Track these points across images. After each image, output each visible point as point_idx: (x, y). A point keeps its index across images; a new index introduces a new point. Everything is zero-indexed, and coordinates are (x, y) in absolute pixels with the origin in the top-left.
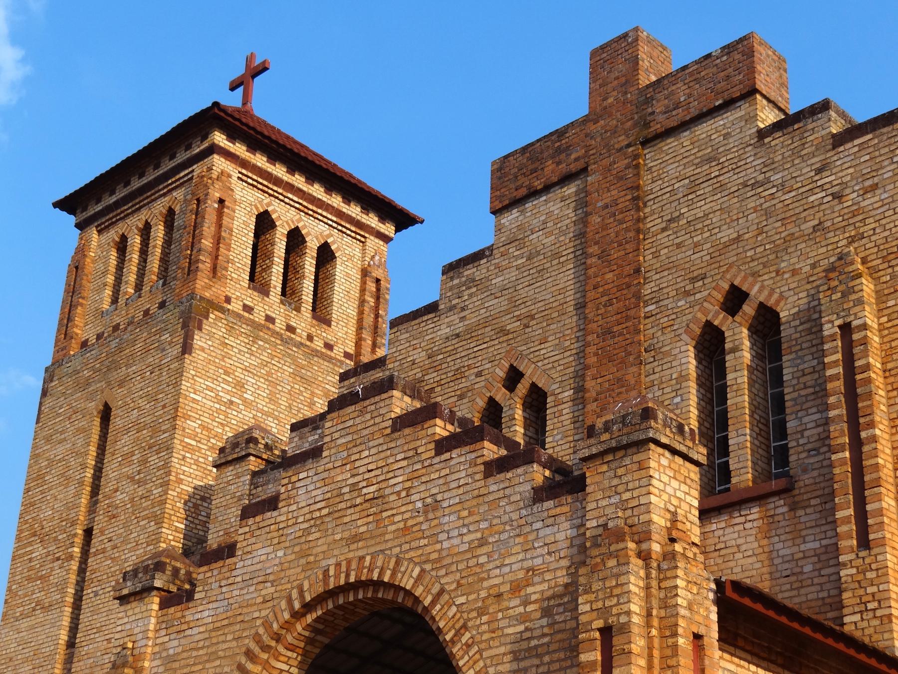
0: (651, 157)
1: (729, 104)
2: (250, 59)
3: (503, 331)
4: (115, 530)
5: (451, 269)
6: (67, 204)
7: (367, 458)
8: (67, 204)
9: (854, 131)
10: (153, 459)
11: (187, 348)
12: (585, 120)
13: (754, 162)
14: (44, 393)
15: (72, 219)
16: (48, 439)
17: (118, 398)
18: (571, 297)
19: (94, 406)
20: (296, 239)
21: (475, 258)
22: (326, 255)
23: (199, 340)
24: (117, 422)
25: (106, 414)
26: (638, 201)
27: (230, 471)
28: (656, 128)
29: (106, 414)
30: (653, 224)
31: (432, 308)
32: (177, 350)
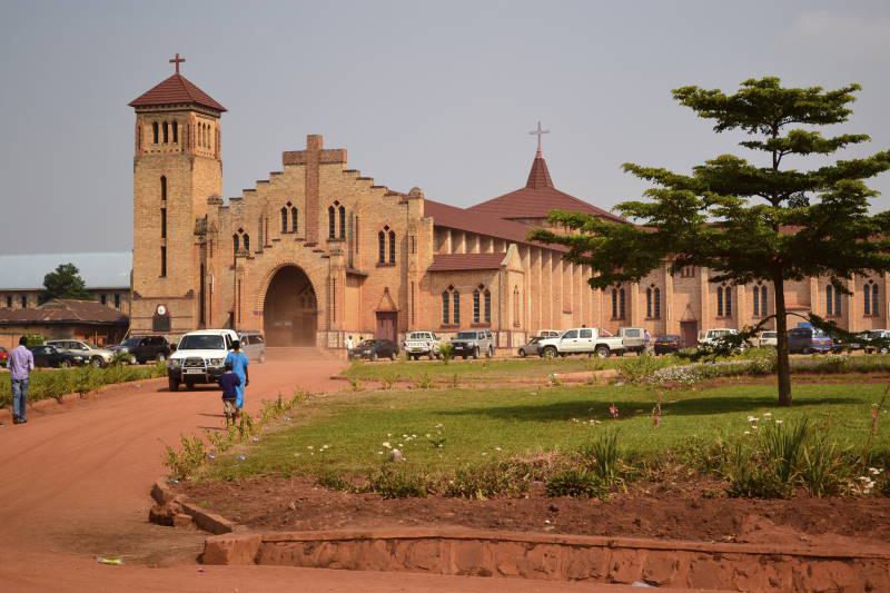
0: (320, 167)
1: (337, 162)
3: (286, 193)
5: (273, 174)
6: (132, 105)
8: (132, 105)
9: (360, 179)
10: (186, 197)
11: (192, 169)
12: (305, 151)
13: (341, 177)
14: (135, 165)
15: (133, 109)
16: (141, 179)
17: (167, 176)
18: (303, 191)
19: (159, 175)
20: (204, 126)
21: (279, 173)
22: (209, 127)
23: (194, 166)
24: (169, 183)
25: (164, 179)
26: (318, 176)
27: (212, 206)
28: (323, 160)
29: (164, 179)
30: (321, 182)
31: (268, 182)
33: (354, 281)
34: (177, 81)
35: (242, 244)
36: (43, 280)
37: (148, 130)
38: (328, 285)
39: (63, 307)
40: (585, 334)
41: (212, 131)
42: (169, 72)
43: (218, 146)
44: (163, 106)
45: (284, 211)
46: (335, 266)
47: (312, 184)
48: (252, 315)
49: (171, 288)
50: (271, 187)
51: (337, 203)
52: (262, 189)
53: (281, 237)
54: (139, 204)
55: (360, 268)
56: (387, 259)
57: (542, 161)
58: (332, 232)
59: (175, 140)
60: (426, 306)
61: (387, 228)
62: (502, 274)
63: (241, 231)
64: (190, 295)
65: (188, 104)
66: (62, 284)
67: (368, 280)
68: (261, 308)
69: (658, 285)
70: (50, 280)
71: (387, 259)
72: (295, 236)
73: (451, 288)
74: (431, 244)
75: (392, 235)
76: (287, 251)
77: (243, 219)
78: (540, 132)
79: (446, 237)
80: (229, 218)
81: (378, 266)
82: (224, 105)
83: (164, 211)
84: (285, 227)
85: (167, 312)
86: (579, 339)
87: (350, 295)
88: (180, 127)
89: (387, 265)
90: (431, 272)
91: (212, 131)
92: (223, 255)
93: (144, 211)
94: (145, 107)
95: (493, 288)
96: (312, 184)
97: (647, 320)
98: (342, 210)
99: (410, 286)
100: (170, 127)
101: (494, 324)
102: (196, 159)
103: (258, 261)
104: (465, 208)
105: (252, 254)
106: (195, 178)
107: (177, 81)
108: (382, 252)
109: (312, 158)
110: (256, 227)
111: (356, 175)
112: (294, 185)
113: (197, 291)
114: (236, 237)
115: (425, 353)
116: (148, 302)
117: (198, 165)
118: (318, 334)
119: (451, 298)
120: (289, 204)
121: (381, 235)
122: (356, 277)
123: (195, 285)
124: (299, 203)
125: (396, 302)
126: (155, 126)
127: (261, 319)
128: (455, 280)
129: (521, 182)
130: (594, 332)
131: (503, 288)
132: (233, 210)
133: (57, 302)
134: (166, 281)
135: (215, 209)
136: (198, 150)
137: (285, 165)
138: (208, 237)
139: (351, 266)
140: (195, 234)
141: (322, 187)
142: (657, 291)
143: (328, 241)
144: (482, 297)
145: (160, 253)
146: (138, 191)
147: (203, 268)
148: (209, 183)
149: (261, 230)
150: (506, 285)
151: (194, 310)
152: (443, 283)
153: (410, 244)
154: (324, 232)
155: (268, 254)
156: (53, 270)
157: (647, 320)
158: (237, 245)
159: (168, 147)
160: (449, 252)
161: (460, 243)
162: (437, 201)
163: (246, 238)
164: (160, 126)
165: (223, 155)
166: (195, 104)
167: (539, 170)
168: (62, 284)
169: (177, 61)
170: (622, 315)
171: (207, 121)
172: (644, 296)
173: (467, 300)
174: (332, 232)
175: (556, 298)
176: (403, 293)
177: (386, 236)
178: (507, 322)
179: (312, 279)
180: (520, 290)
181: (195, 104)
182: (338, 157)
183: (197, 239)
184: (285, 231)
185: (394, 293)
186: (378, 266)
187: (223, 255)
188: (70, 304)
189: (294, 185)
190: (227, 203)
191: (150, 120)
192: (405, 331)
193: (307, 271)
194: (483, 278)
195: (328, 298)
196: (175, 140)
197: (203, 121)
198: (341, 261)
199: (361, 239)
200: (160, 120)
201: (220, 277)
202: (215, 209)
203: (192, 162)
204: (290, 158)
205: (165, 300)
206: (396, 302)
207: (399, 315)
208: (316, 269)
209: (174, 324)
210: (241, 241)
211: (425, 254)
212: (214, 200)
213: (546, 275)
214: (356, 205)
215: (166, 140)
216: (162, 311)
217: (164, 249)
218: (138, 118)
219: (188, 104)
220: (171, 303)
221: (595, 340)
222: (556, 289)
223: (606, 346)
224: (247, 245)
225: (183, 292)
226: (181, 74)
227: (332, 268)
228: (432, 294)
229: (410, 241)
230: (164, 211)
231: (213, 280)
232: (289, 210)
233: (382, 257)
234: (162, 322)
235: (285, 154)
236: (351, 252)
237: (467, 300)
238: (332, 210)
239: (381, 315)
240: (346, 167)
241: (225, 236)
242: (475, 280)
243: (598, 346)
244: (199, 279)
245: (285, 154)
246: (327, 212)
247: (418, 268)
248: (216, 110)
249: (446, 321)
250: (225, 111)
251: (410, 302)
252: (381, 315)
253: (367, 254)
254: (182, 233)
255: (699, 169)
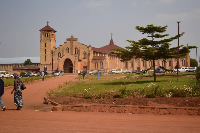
0: (73, 41)
2: (48, 22)
4: (48, 49)
6: (40, 31)
7: (68, 55)
12: (71, 39)
14: (40, 41)
15: (40, 31)
17: (46, 43)
19: (45, 43)
25: (45, 44)
29: (45, 44)
32: (50, 42)
33: (79, 61)
34: (48, 26)
35: (59, 55)
36: (24, 62)
37: (43, 35)
38: (75, 62)
39: (28, 66)
40: (120, 70)
41: (54, 35)
42: (46, 25)
43: (55, 38)
44: (45, 31)
45: (67, 49)
46: (76, 59)
47: (72, 44)
48: (61, 67)
49: (47, 63)
50: (64, 45)
51: (76, 48)
52: (63, 45)
53: (66, 54)
54: (41, 48)
55: (80, 59)
56: (85, 57)
57: (112, 40)
58: (75, 53)
59: (47, 37)
60: (92, 65)
61: (85, 52)
62: (105, 60)
63: (59, 53)
64: (50, 64)
65: (50, 30)
66: (28, 62)
67: (82, 61)
68: (63, 66)
69: (133, 61)
70: (26, 62)
71: (85, 57)
72: (69, 53)
73: (96, 62)
74: (93, 55)
75: (86, 53)
76: (67, 56)
77: (59, 50)
78: (111, 35)
79: (95, 53)
80: (57, 50)
81: (83, 58)
82: (56, 31)
83: (46, 49)
84: (67, 52)
85: (46, 67)
86: (119, 71)
87: (79, 64)
88: (48, 34)
89: (85, 58)
90: (93, 59)
91: (54, 35)
92: (56, 57)
93: (42, 49)
94: (42, 31)
95: (104, 62)
96: (72, 44)
97: (131, 67)
98: (77, 49)
99: (89, 62)
100: (46, 35)
101: (104, 69)
102: (51, 40)
103: (62, 58)
104: (99, 48)
105: (61, 57)
106: (51, 43)
107: (48, 26)
108: (84, 56)
109: (72, 40)
110: (62, 51)
111: (79, 43)
112: (69, 44)
113: (52, 63)
114: (58, 54)
115: (92, 74)
116: (43, 65)
117: (52, 41)
118: (73, 71)
119: (96, 64)
120: (68, 48)
121: (84, 53)
122: (80, 61)
123: (51, 62)
124: (69, 48)
125: (87, 65)
126: (44, 34)
127: (63, 68)
128: (97, 61)
129: (108, 43)
130: (122, 70)
131: (106, 62)
132: (58, 49)
133: (27, 66)
134: (46, 62)
135: (55, 49)
136: (52, 38)
137: (67, 41)
138: (53, 54)
139: (79, 59)
140: (51, 53)
141: (73, 45)
142: (133, 62)
143: (75, 54)
144: (102, 64)
145: (45, 57)
146: (41, 46)
147: (53, 59)
148: (53, 44)
149: (63, 53)
150: (106, 61)
151: (51, 67)
152: (95, 61)
153: (89, 55)
154: (74, 53)
155: (64, 57)
156: (26, 60)
157: (131, 67)
158: (58, 55)
159: (46, 38)
160: (96, 56)
161: (98, 54)
162: (105, 46)
163: (60, 54)
164: (45, 34)
165: (56, 39)
166: (51, 30)
167: (112, 41)
168: (28, 62)
169: (48, 23)
170: (126, 67)
171: (53, 33)
172: (130, 63)
173: (99, 64)
174: (75, 53)
175: (115, 64)
176: (88, 63)
177: (85, 53)
178: (106, 68)
179: (72, 61)
180: (109, 62)
181: (51, 30)
182: (76, 39)
183: (51, 54)
184: (67, 53)
185: (86, 63)
186: (83, 58)
187: (56, 57)
188: (29, 66)
189: (69, 44)
190: (57, 48)
191: (43, 33)
192: (88, 70)
193: (71, 60)
194: (102, 60)
195: (75, 64)
196: (47, 37)
197: (52, 33)
198: (77, 58)
199: (80, 54)
200: (45, 33)
201: (56, 61)
202: (55, 49)
203: (50, 41)
204: (68, 40)
205: (46, 65)
206: (87, 65)
207: (87, 67)
208: (72, 59)
209: (48, 69)
210: (59, 54)
211: (92, 56)
212: (54, 47)
213: (113, 60)
214: (80, 48)
215: (46, 37)
216: (45, 67)
217: (46, 56)
218: (41, 33)
219: (50, 30)
220: (47, 65)
221: (122, 71)
222: (115, 62)
223: (124, 72)
224: (60, 55)
225: (49, 64)
226: (48, 25)
227: (75, 59)
228: (93, 63)
229: (89, 54)
230: (46, 49)
231: (54, 61)
232: (68, 49)
233: (84, 57)
234: (46, 69)
235: (67, 39)
236: (79, 56)
237: (99, 64)
238: (75, 49)
239: (84, 67)
240: (78, 41)
241: (57, 53)
242: (100, 61)
243: (122, 72)
244: (52, 61)
245: (67, 39)
246: (74, 49)
247: (91, 59)
248: (54, 31)
249: (96, 68)
250: (56, 31)
251: (89, 65)
252: (84, 67)
253: (82, 56)
254: (49, 53)
255: (140, 41)
